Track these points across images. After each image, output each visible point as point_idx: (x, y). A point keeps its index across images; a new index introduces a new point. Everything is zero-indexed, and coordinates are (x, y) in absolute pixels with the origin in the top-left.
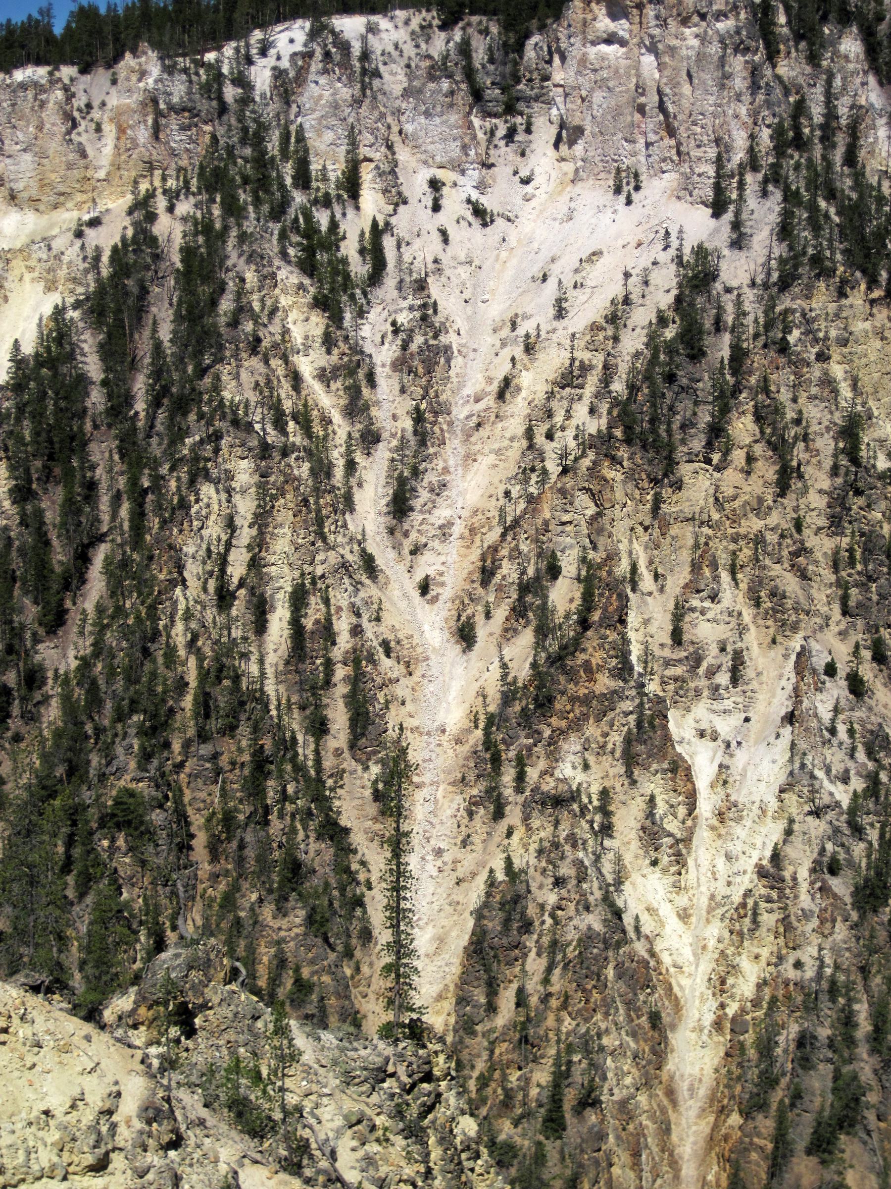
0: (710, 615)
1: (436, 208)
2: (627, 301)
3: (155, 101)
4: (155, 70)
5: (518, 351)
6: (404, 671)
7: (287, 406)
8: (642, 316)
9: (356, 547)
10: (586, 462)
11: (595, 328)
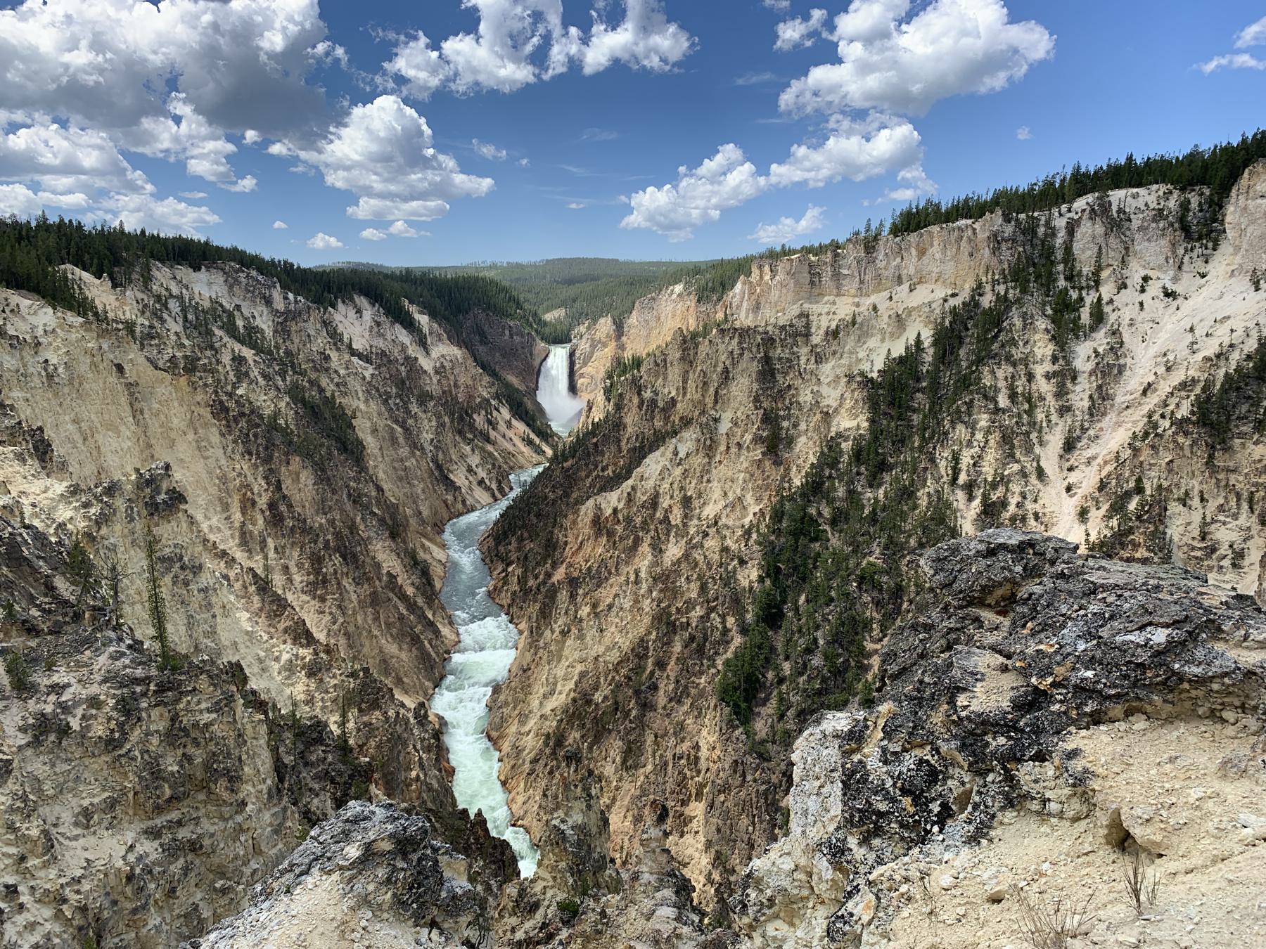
0: (1229, 526)
1: (1143, 291)
2: (1231, 346)
3: (995, 236)
4: (1000, 221)
5: (1161, 370)
6: (1043, 528)
7: (1020, 390)
8: (1235, 356)
9: (1035, 464)
10: (1170, 432)
11: (1207, 359)
